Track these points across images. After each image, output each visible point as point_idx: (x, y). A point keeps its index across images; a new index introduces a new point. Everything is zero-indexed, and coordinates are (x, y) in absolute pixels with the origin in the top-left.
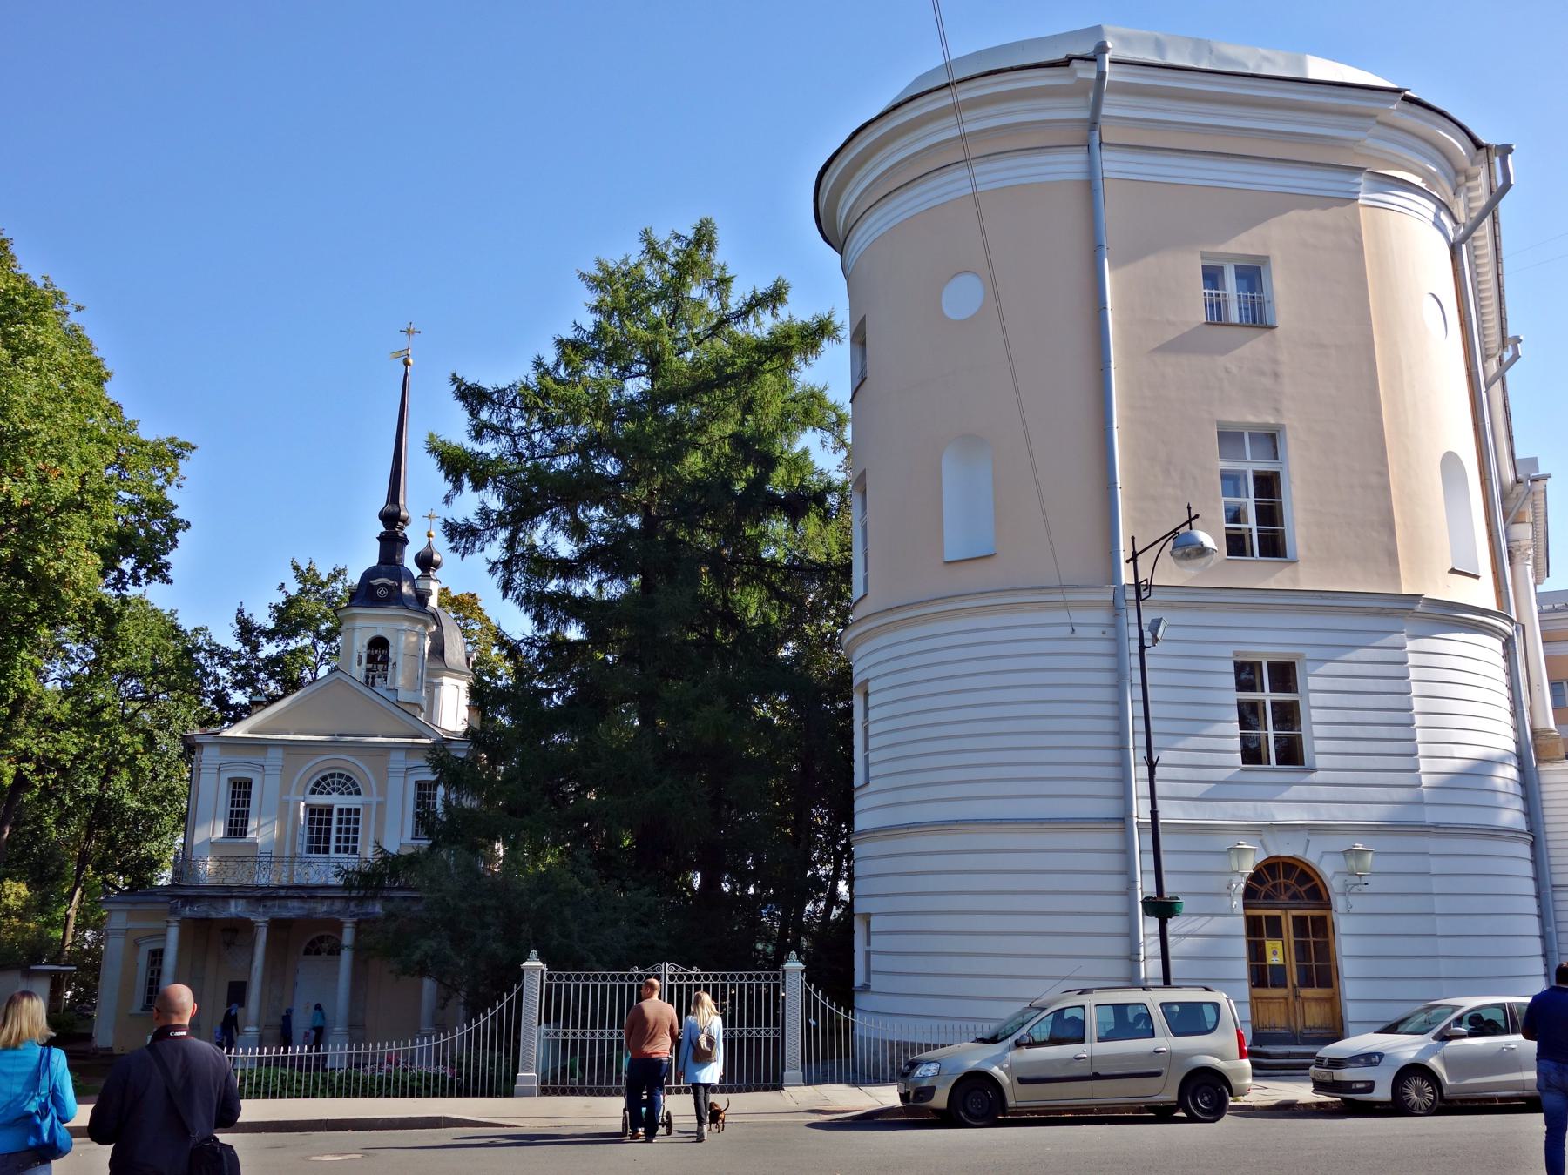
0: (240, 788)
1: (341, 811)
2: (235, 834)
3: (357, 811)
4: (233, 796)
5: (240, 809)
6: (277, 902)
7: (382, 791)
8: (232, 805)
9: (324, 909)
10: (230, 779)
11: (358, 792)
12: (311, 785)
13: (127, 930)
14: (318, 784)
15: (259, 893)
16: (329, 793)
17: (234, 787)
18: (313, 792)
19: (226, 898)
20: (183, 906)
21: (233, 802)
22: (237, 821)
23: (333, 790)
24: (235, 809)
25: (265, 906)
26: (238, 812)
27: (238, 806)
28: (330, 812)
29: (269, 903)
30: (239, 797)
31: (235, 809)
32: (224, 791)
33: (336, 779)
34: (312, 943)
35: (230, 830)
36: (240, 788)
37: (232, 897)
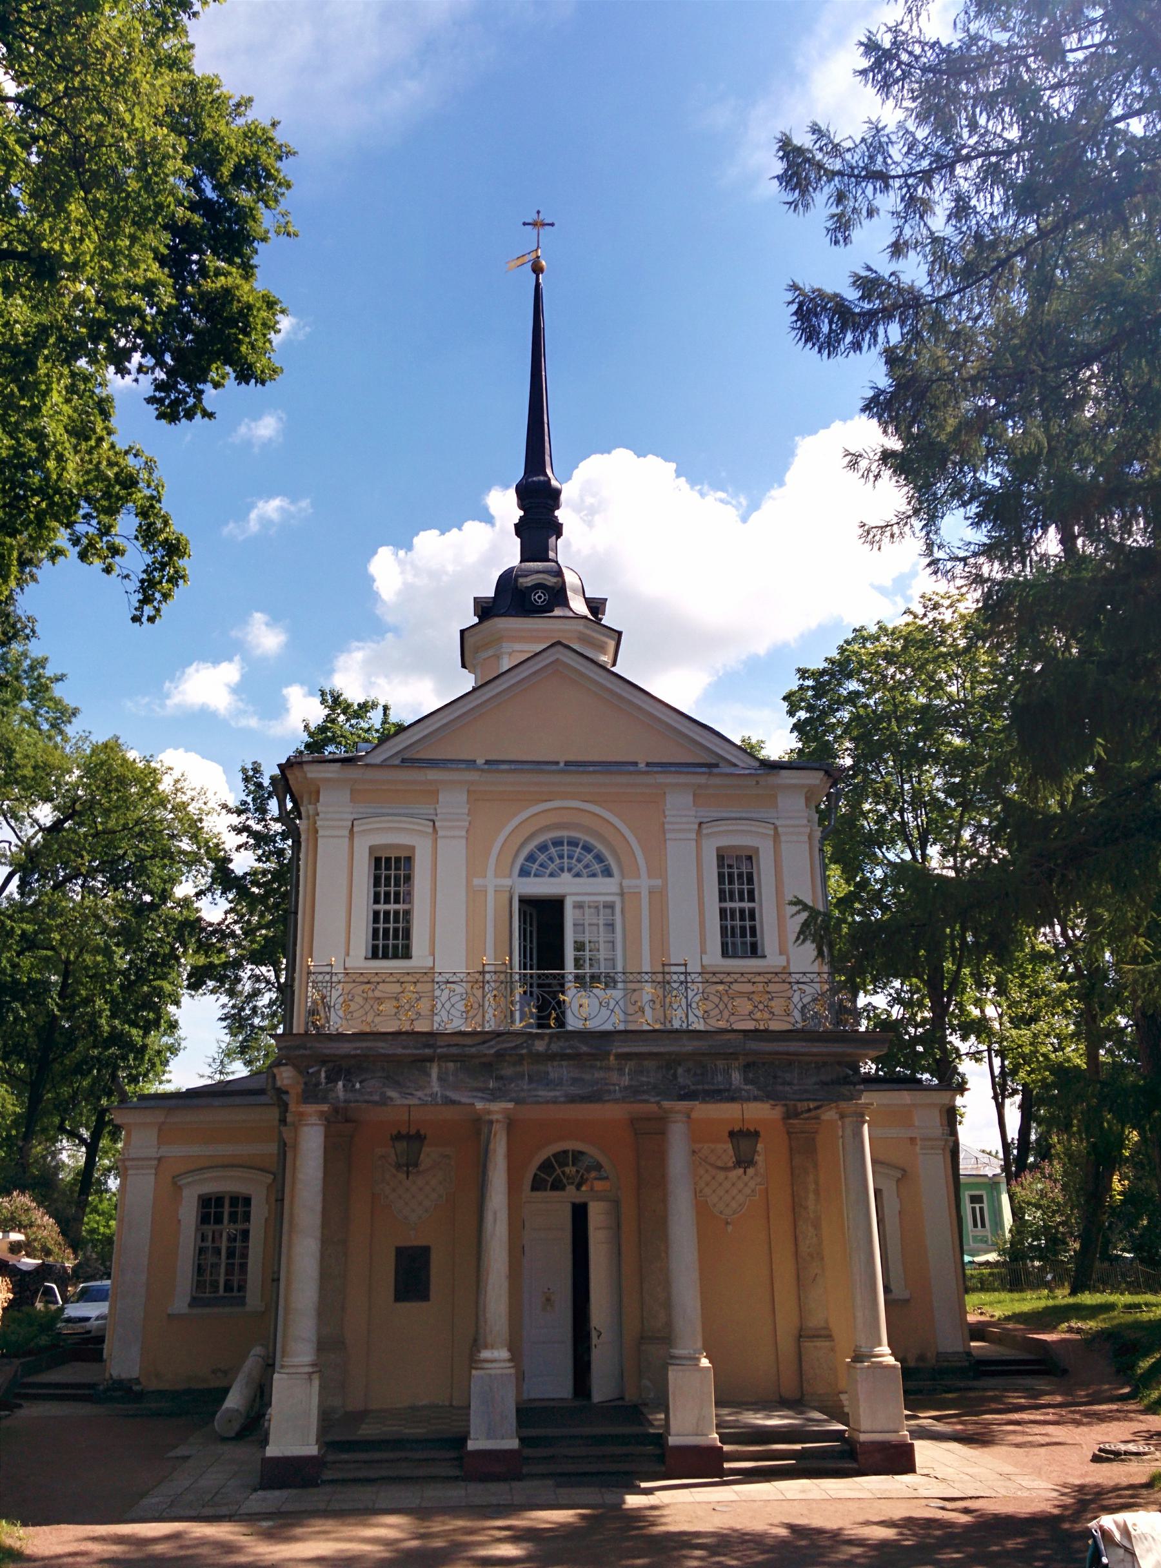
0: (388, 868)
1: (579, 906)
3: (610, 906)
4: (377, 883)
5: (392, 907)
6: (525, 1068)
7: (658, 869)
8: (376, 901)
9: (625, 1081)
10: (372, 849)
11: (608, 873)
12: (521, 860)
13: (160, 1159)
14: (531, 858)
15: (490, 1050)
16: (551, 875)
17: (377, 866)
18: (524, 873)
19: (420, 1063)
20: (332, 1079)
22: (386, 931)
23: (562, 870)
24: (382, 907)
25: (499, 1078)
26: (387, 913)
27: (387, 901)
29: (508, 1071)
30: (388, 884)
31: (382, 907)
34: (546, 1166)
35: (375, 949)
36: (388, 868)
37: (430, 1059)
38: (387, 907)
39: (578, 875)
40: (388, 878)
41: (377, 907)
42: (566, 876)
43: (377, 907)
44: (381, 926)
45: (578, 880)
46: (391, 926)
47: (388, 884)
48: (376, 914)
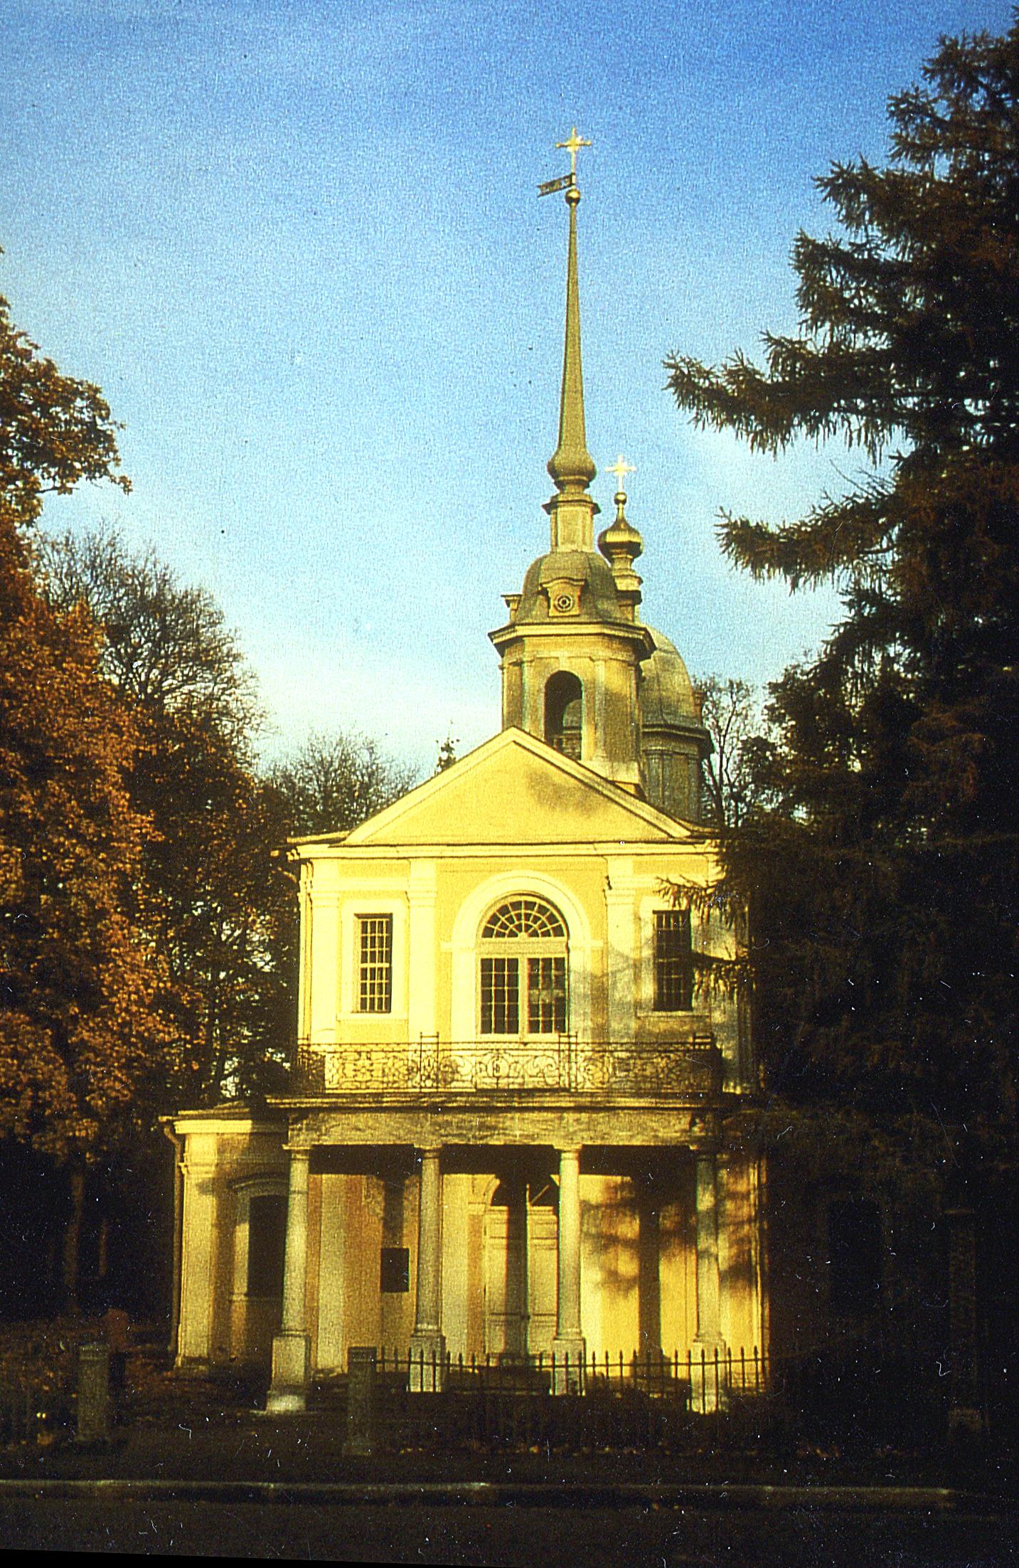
2: (372, 1007)
5: (377, 965)
8: (364, 961)
14: (494, 920)
16: (513, 934)
18: (488, 933)
21: (364, 954)
22: (372, 985)
24: (369, 965)
26: (373, 970)
27: (373, 961)
28: (514, 963)
30: (373, 946)
31: (369, 965)
32: (353, 932)
33: (523, 911)
35: (363, 1000)
38: (373, 965)
39: (535, 934)
40: (373, 939)
41: (364, 965)
42: (523, 935)
43: (364, 965)
44: (368, 982)
45: (534, 939)
46: (377, 981)
47: (373, 946)
48: (364, 971)
